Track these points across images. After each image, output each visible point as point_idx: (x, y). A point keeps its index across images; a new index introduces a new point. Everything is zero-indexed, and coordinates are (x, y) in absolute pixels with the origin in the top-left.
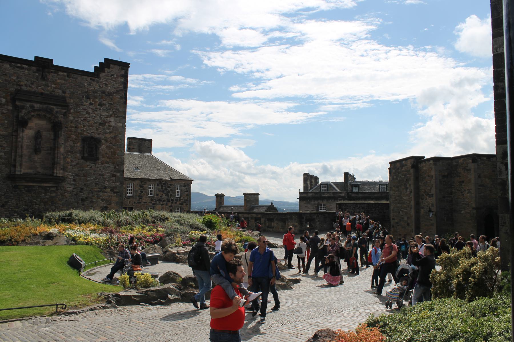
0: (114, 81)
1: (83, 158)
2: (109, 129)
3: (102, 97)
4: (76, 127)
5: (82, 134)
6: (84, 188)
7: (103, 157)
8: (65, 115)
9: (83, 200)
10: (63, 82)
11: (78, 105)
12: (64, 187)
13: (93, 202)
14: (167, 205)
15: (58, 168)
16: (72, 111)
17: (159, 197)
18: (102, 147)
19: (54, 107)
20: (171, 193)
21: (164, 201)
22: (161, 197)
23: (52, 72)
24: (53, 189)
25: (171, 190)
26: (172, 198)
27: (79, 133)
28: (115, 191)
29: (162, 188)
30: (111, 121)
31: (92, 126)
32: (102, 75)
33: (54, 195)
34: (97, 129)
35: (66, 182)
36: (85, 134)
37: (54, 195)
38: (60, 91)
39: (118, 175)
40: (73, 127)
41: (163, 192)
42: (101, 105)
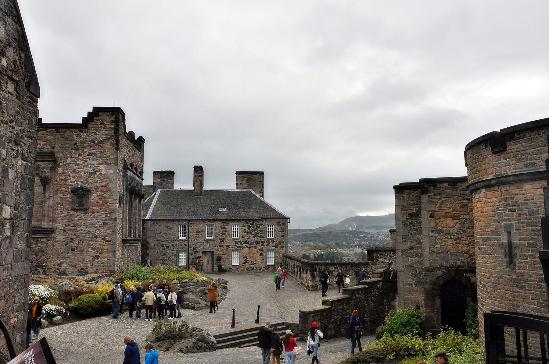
0: (104, 128)
1: (74, 209)
2: (99, 178)
3: (91, 147)
4: (66, 180)
5: (72, 185)
6: (74, 237)
7: (94, 206)
8: (52, 169)
9: (73, 250)
10: (52, 137)
11: (67, 158)
12: (54, 238)
13: (83, 251)
14: (255, 248)
15: (46, 220)
16: (61, 164)
17: (246, 239)
18: (92, 197)
19: (41, 163)
20: (261, 234)
21: (252, 243)
22: (249, 238)
23: (41, 130)
24: (43, 240)
25: (261, 230)
26: (262, 240)
27: (68, 185)
28: (107, 240)
29: (249, 229)
30: (101, 170)
31: (81, 176)
32: (91, 125)
33: (44, 245)
34: (87, 179)
35: (57, 233)
36: (75, 185)
37: (44, 245)
38: (49, 147)
39: (110, 223)
40: (63, 180)
41: (251, 233)
42: (90, 154)
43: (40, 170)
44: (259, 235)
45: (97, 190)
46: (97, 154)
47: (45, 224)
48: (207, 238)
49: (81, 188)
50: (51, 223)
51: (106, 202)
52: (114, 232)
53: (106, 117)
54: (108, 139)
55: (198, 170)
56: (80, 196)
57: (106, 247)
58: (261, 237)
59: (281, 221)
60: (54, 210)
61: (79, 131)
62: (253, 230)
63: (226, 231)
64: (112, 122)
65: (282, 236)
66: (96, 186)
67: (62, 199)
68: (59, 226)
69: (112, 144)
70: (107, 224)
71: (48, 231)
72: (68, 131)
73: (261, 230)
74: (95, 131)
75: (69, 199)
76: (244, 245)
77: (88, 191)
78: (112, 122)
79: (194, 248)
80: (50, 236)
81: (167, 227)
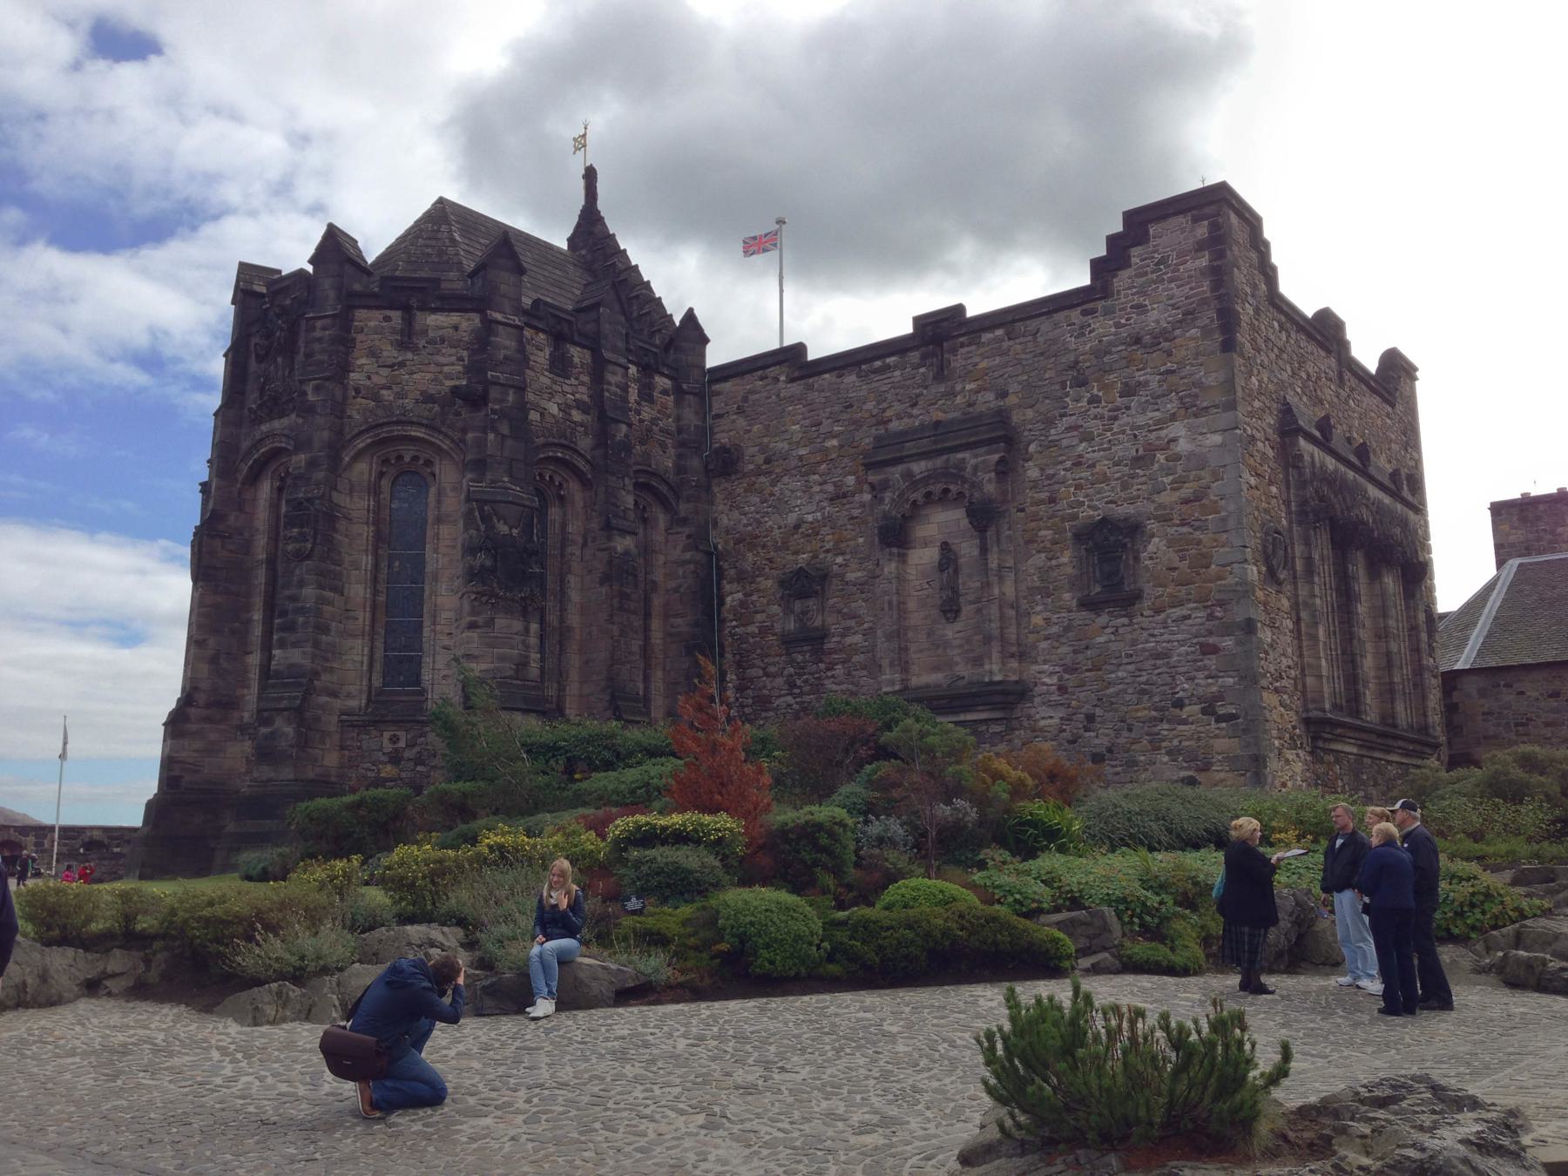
0: (1171, 280)
2: (1169, 471)
3: (1130, 361)
4: (1052, 500)
5: (1074, 517)
6: (1098, 711)
8: (1004, 470)
9: (1098, 758)
10: (997, 360)
11: (1049, 422)
12: (1029, 717)
13: (1135, 763)
16: (1032, 448)
18: (1151, 548)
23: (962, 345)
27: (1063, 520)
28: (1221, 711)
30: (1174, 440)
32: (1122, 280)
35: (1037, 700)
36: (1085, 513)
38: (990, 396)
39: (1228, 643)
40: (1042, 502)
42: (1129, 391)
43: (965, 481)
45: (1165, 519)
46: (1154, 385)
47: (995, 668)
49: (1104, 521)
50: (1014, 664)
51: (1204, 561)
52: (1250, 679)
53: (1168, 237)
54: (1189, 316)
56: (1108, 548)
57: (1221, 744)
60: (1023, 616)
61: (1085, 313)
64: (1200, 247)
66: (1161, 506)
68: (1044, 674)
70: (1213, 650)
71: (1005, 693)
72: (1044, 325)
74: (1137, 300)
75: (1069, 570)
77: (1133, 529)
78: (1200, 247)
81: (1555, 695)
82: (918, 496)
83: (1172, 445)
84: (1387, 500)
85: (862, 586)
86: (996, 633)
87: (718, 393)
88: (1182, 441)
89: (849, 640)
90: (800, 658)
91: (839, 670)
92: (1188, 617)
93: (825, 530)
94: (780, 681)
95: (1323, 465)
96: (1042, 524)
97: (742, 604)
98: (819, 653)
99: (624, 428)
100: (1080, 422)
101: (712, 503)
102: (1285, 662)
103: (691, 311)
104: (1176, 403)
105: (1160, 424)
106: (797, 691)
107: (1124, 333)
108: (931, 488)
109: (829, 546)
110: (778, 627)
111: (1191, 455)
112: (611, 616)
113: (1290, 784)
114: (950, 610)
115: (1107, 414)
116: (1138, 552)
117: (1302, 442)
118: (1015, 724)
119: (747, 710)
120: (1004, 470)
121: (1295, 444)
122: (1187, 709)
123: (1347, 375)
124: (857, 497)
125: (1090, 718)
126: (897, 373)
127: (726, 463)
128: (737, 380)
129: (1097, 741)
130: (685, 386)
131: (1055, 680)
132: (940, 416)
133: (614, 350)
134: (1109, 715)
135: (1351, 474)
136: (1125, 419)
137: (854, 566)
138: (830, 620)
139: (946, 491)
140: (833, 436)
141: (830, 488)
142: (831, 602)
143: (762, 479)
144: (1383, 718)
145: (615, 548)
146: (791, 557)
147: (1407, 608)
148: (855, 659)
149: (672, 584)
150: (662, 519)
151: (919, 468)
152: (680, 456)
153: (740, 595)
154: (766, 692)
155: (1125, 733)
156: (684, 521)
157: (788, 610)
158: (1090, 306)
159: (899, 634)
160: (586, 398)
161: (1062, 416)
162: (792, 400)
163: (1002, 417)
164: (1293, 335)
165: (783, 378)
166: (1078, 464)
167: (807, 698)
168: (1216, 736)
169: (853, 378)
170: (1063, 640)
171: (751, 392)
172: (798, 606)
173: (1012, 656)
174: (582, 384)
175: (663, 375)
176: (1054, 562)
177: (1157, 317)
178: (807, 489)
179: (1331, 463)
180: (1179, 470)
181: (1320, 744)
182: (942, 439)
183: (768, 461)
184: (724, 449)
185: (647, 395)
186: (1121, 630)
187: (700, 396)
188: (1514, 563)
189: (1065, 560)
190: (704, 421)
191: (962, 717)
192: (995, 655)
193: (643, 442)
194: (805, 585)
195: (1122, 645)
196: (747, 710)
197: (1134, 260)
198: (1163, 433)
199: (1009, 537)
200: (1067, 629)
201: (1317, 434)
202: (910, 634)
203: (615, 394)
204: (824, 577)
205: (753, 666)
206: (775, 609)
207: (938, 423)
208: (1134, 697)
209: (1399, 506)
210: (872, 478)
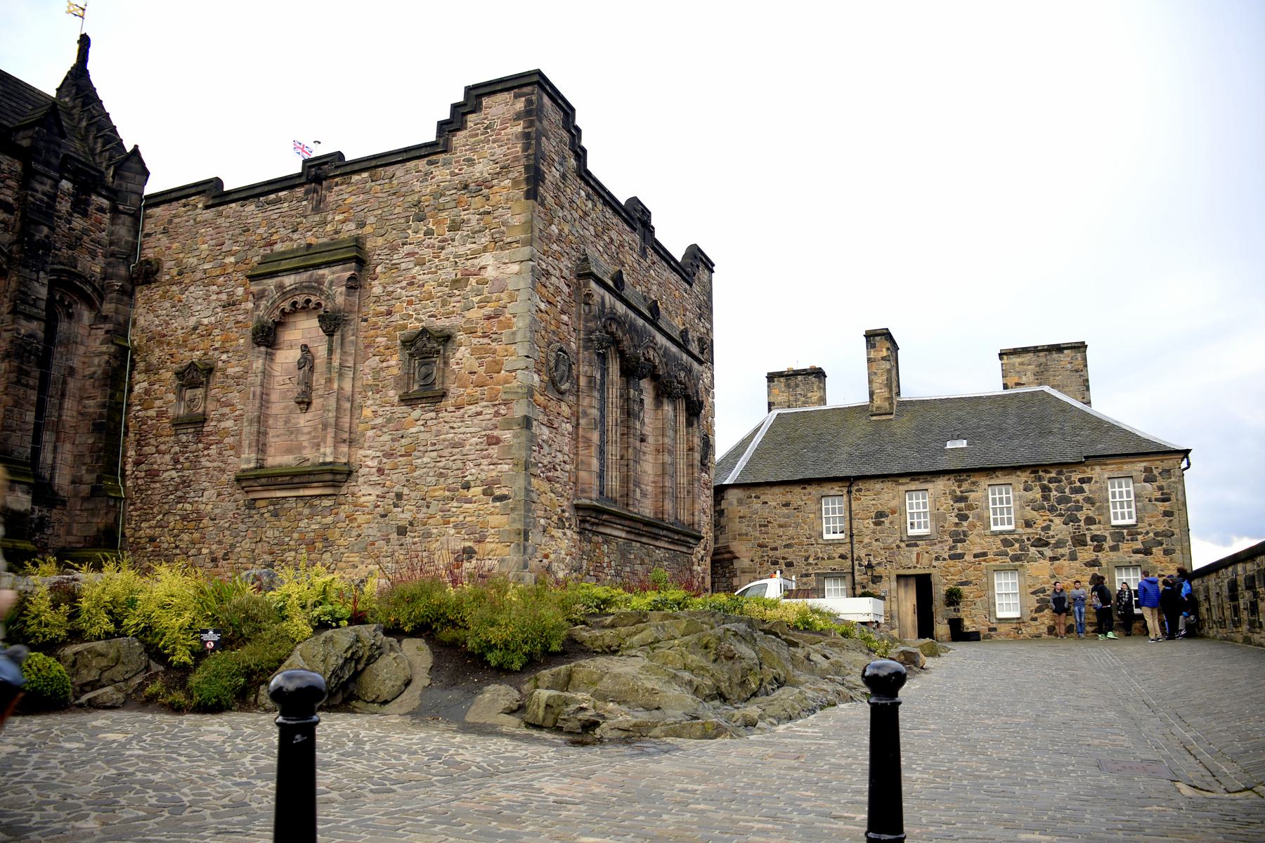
1: (408, 400)
3: (458, 203)
4: (389, 313)
5: (404, 327)
6: (406, 491)
8: (354, 285)
9: (402, 531)
11: (394, 249)
12: (353, 495)
13: (429, 535)
14: (1073, 557)
16: (379, 269)
17: (1036, 531)
18: (458, 355)
21: (1060, 544)
22: (1047, 528)
24: (327, 503)
25: (1088, 500)
26: (1096, 530)
27: (395, 329)
29: (1046, 498)
31: (430, 297)
32: (459, 139)
33: (329, 519)
35: (361, 480)
37: (329, 519)
38: (352, 226)
39: (507, 435)
40: (381, 314)
41: (1052, 509)
42: (454, 227)
43: (322, 292)
44: (1081, 516)
45: (472, 332)
46: (474, 222)
48: (911, 532)
49: (424, 331)
50: (344, 448)
51: (496, 367)
55: (879, 339)
57: (495, 520)
58: (1090, 521)
59: (1158, 465)
61: (430, 163)
62: (1060, 501)
63: (970, 508)
64: (518, 117)
65: (1166, 514)
66: (469, 321)
67: (376, 372)
68: (367, 458)
69: (516, 183)
71: (333, 472)
72: (399, 170)
73: (1088, 500)
74: (470, 155)
75: (395, 371)
76: (1033, 550)
79: (870, 566)
80: (344, 490)
81: (787, 505)
82: (286, 305)
83: (483, 272)
84: (674, 349)
85: (238, 379)
86: (332, 421)
87: (151, 217)
88: (489, 268)
89: (223, 425)
90: (184, 438)
91: (214, 450)
92: (479, 414)
93: (217, 331)
94: (168, 457)
95: (612, 308)
96: (379, 332)
97: (147, 392)
98: (199, 435)
99: (46, 230)
100: (416, 250)
101: (133, 306)
102: (560, 457)
103: (136, 147)
104: (488, 238)
105: (475, 254)
106: (179, 466)
107: (457, 180)
108: (297, 298)
109: (217, 345)
110: (171, 412)
111: (496, 279)
112: (6, 388)
113: (552, 556)
114: (304, 403)
115: (437, 244)
116: (448, 358)
117: (593, 284)
118: (342, 499)
119: (140, 482)
120: (354, 285)
121: (586, 286)
122: (472, 490)
123: (650, 251)
124: (243, 306)
125: (399, 496)
126: (286, 205)
127: (148, 274)
128: (165, 206)
129: (402, 516)
130: (121, 207)
131: (375, 463)
132: (313, 241)
133: (47, 164)
134: (413, 494)
135: (640, 322)
136: (449, 249)
137: (234, 362)
138: (210, 407)
139: (308, 301)
140: (230, 253)
141: (224, 297)
142: (213, 392)
143: (174, 288)
144: (656, 513)
145: (18, 331)
146: (188, 354)
147: (688, 433)
148: (226, 440)
149: (89, 371)
150: (87, 316)
151: (289, 281)
152: (108, 264)
153: (145, 384)
154: (155, 467)
155: (424, 510)
156: (105, 319)
157: (180, 398)
158: (434, 158)
159: (261, 420)
160: (10, 200)
161: (404, 244)
162: (205, 223)
163: (358, 243)
164: (600, 206)
165: (200, 205)
166: (411, 284)
167: (186, 473)
168: (491, 514)
169: (253, 207)
170: (385, 430)
171: (175, 216)
172: (189, 394)
173: (344, 441)
174: (9, 187)
175: (100, 195)
176: (385, 364)
177: (482, 169)
178: (207, 298)
179: (621, 308)
180: (485, 292)
181: (587, 526)
182: (310, 259)
183: (180, 273)
184: (148, 262)
185: (80, 206)
186: (429, 423)
187: (136, 217)
188: (775, 412)
189: (393, 362)
190: (136, 236)
191: (301, 492)
192: (330, 440)
193: (70, 247)
194: (196, 376)
195: (428, 435)
196: (140, 482)
197: (469, 124)
198: (476, 262)
199: (352, 342)
200: (389, 421)
201: (611, 283)
202: (271, 422)
203: (42, 201)
204: (210, 371)
205: (148, 444)
206: (171, 397)
207: (309, 246)
208: (434, 479)
209: (685, 356)
210: (255, 288)
